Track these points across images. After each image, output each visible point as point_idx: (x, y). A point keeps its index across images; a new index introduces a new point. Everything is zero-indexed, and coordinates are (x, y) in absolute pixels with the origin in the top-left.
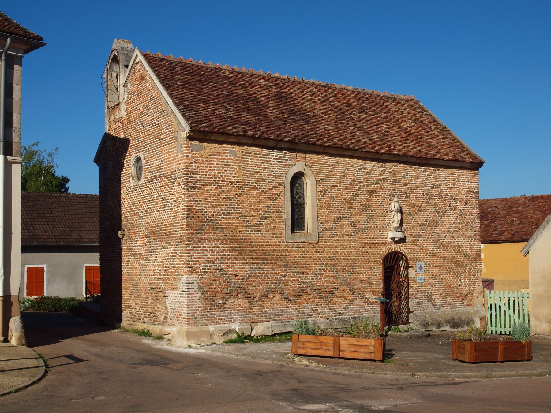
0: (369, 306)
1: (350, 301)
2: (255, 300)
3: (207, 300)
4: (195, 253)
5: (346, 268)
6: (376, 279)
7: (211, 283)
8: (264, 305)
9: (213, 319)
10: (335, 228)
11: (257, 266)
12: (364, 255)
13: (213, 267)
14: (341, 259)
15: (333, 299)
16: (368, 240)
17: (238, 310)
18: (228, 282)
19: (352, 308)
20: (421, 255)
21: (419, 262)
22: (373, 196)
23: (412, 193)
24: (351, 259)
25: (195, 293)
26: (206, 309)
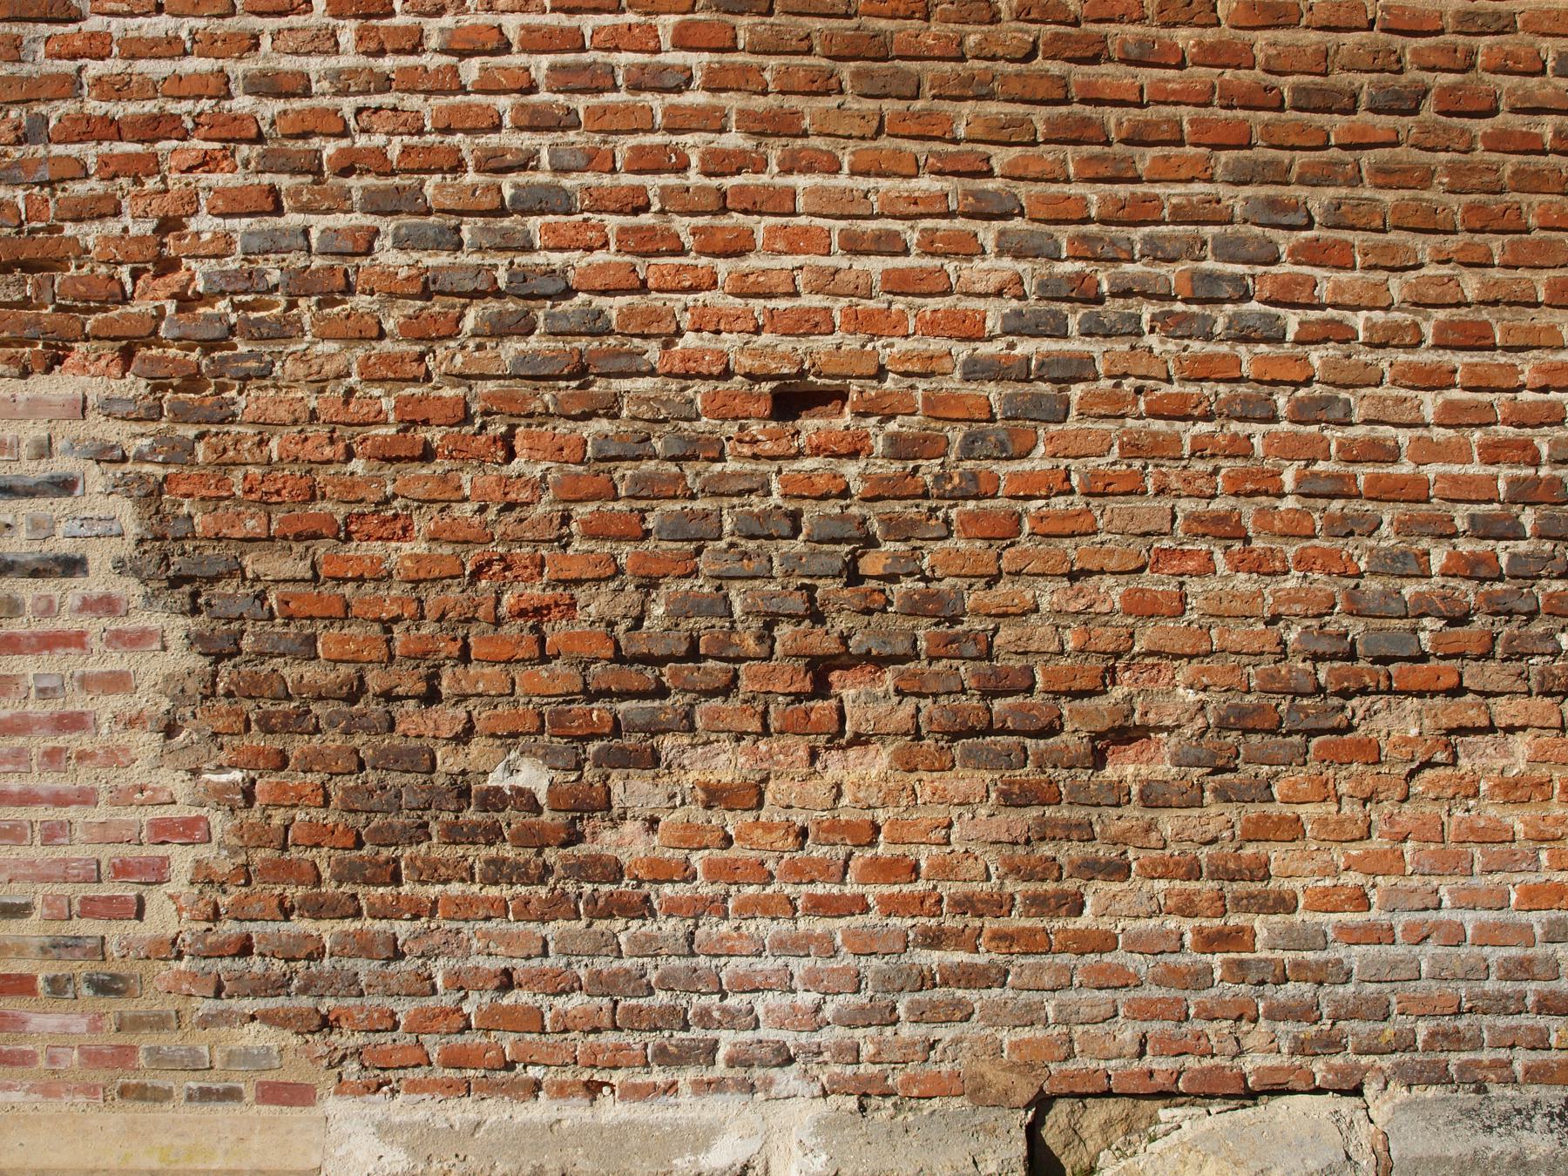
2: (1124, 768)
3: (298, 746)
4: (98, 47)
7: (349, 491)
8: (1276, 853)
9: (405, 1009)
11: (1158, 253)
13: (388, 256)
17: (821, 906)
18: (647, 490)
25: (96, 626)
26: (283, 871)
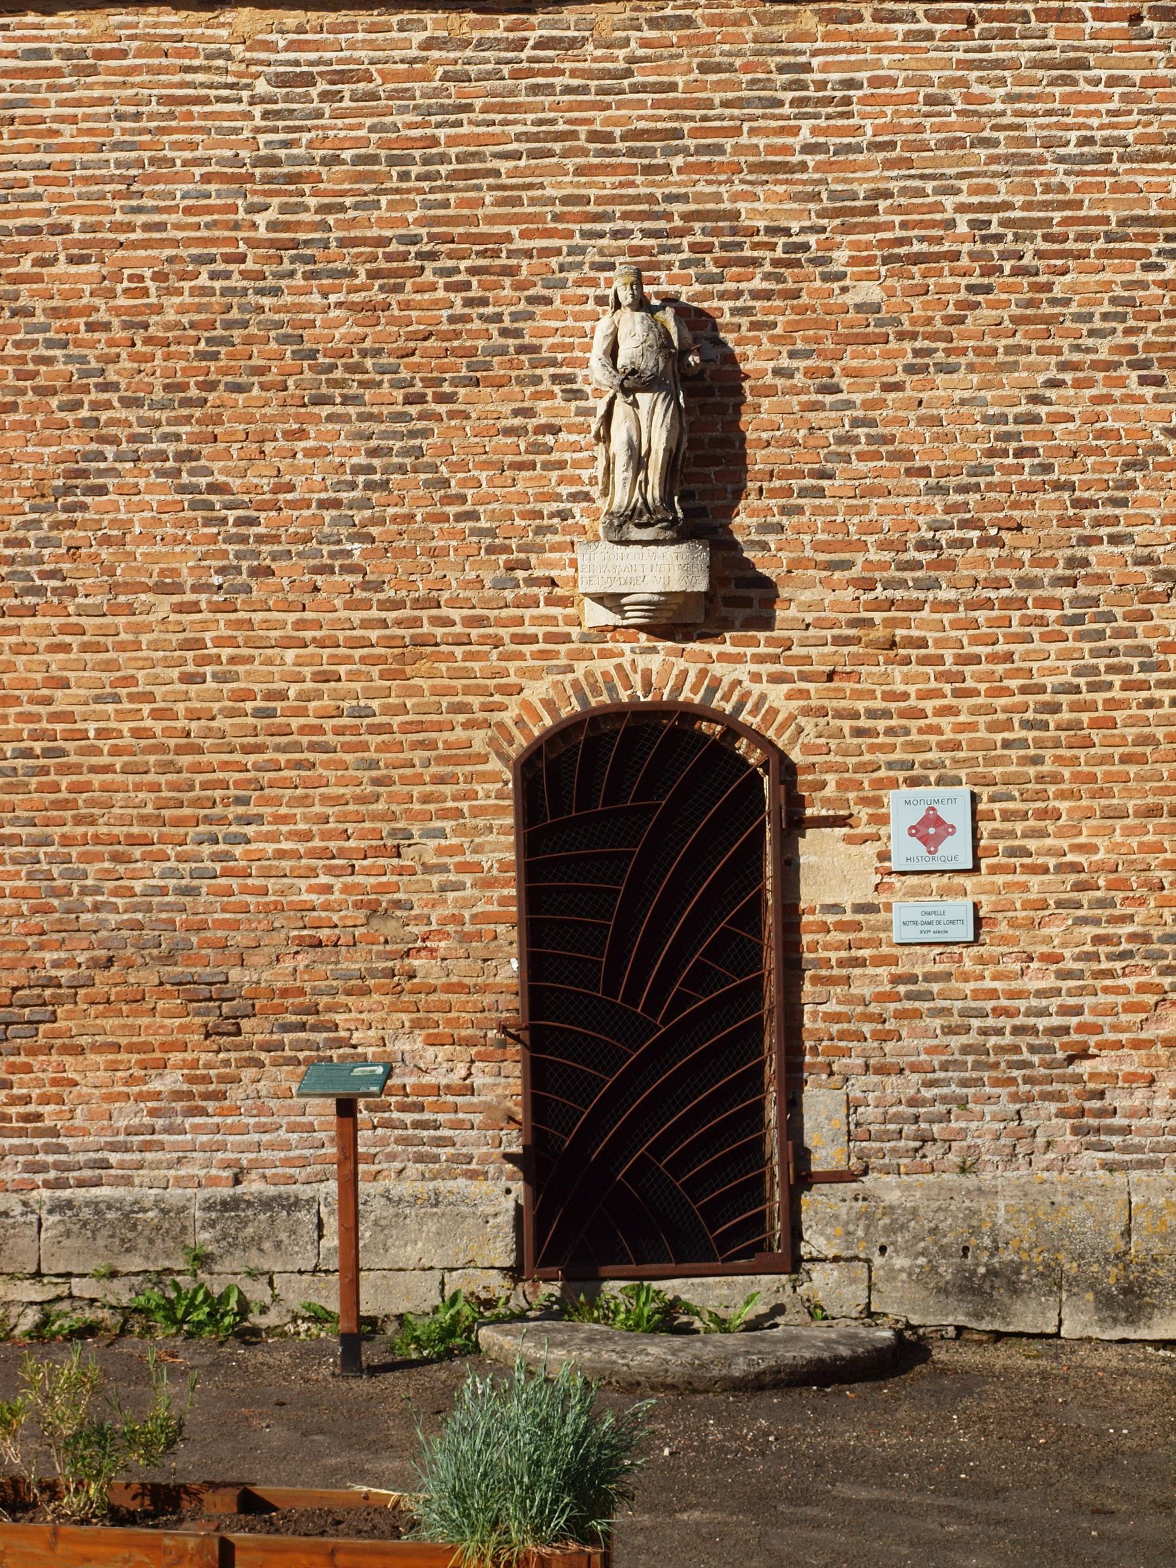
0: (388, 1124)
1: (191, 1080)
5: (154, 832)
6: (457, 919)
10: (42, 543)
12: (330, 738)
14: (108, 769)
15: (36, 1062)
16: (366, 624)
19: (218, 1129)
20: (945, 722)
21: (913, 782)
22: (428, 276)
23: (846, 229)
24: (197, 769)
